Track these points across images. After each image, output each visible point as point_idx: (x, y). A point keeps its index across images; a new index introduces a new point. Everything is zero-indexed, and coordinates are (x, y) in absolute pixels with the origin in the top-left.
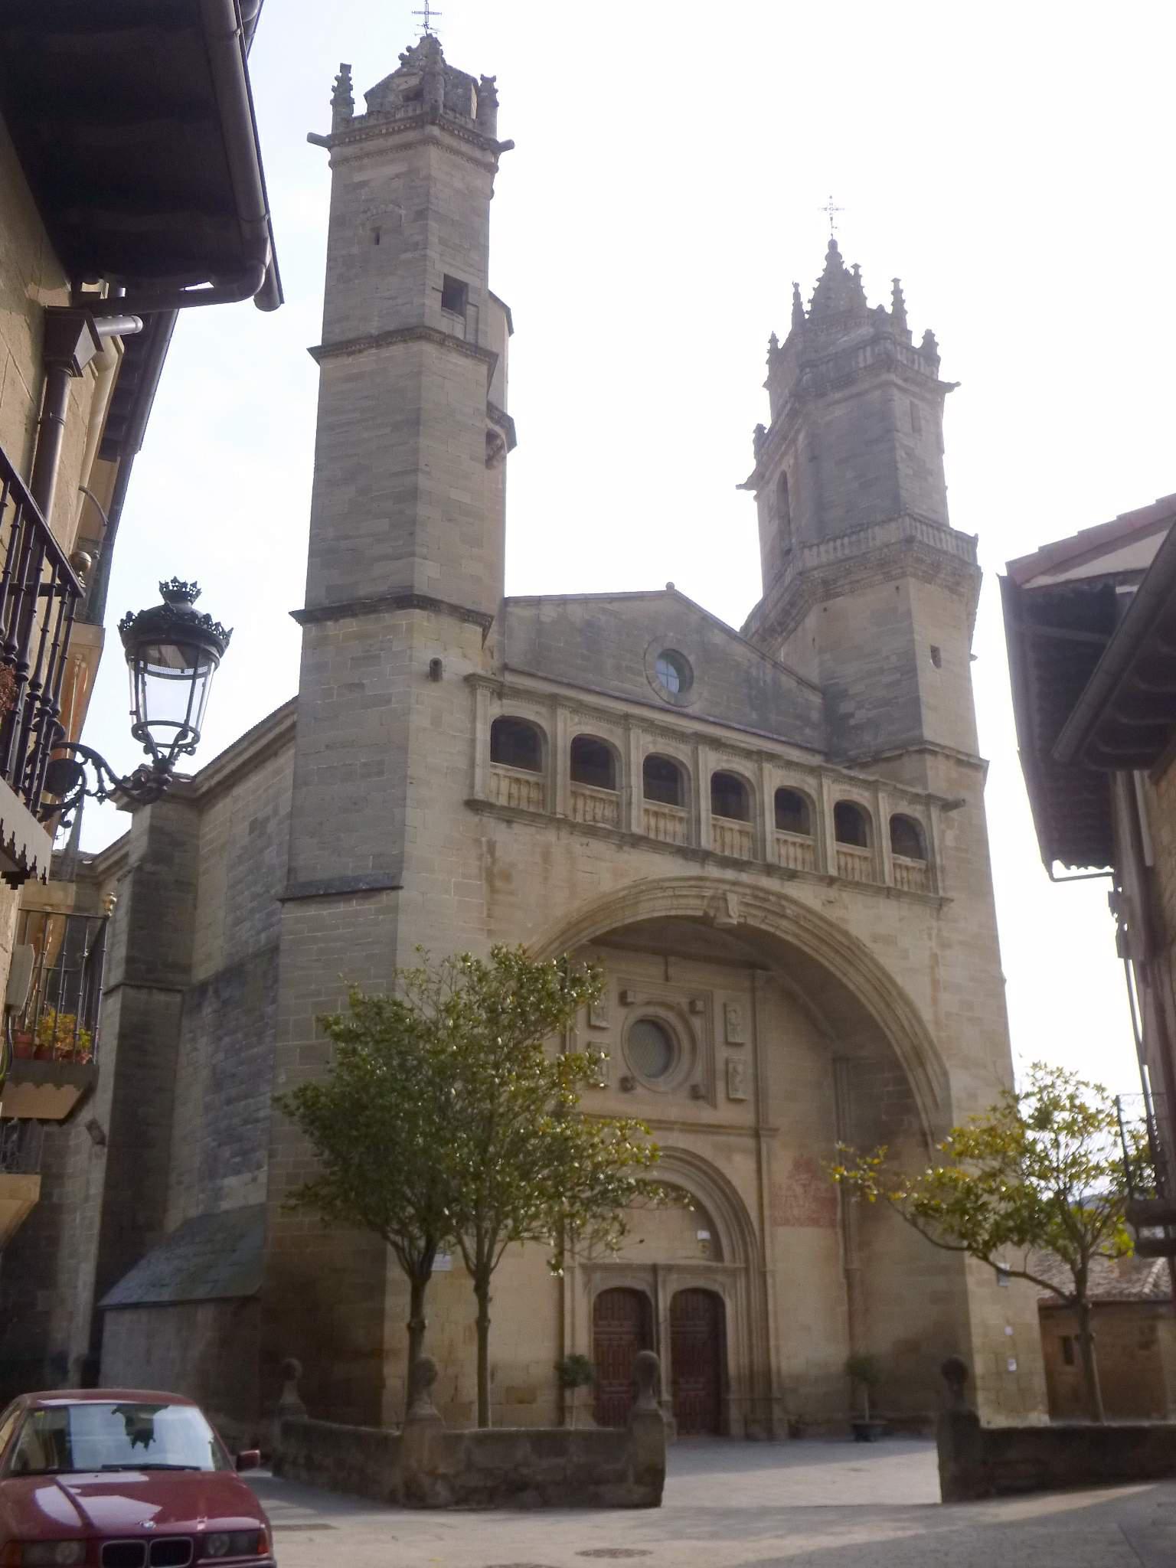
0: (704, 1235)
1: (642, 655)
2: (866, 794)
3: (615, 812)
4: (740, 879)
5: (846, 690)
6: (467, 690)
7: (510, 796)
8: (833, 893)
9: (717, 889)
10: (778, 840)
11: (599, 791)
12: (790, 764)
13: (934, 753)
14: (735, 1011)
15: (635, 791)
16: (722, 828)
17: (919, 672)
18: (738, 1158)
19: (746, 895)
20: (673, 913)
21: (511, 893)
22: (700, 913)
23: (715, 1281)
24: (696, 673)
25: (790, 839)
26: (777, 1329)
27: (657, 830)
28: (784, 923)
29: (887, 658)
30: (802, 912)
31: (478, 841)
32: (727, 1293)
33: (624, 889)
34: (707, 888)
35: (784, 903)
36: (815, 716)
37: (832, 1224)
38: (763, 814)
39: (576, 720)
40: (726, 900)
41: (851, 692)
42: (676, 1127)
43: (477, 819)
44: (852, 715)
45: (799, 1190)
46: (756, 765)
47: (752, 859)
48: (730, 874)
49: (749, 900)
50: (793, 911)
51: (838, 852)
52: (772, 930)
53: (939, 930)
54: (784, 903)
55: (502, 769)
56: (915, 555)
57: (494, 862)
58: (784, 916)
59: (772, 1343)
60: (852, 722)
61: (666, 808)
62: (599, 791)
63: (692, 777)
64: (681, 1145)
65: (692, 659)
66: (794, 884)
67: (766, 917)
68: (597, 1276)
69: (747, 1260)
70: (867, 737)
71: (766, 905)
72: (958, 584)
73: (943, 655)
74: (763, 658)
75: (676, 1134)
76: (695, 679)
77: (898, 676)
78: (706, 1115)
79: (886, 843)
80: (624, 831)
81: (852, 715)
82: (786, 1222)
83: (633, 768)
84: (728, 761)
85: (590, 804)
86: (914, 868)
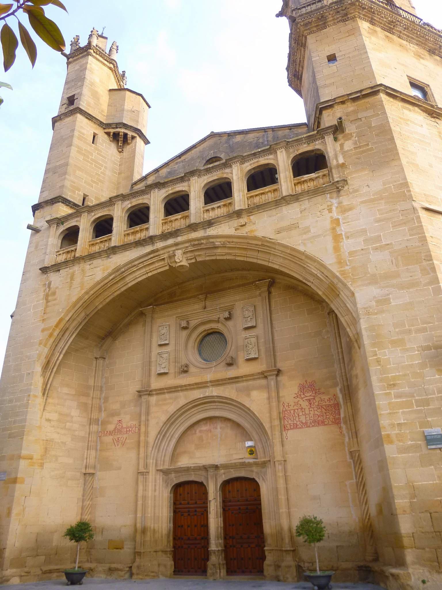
4: (177, 241)
9: (169, 252)
18: (255, 394)
19: (187, 247)
20: (150, 274)
21: (55, 299)
22: (167, 268)
23: (252, 471)
28: (219, 251)
30: (223, 240)
33: (110, 275)
35: (211, 240)
37: (337, 422)
42: (208, 385)
43: (46, 276)
45: (305, 404)
48: (171, 241)
49: (190, 249)
50: (220, 242)
52: (214, 258)
54: (211, 240)
56: (302, 24)
58: (216, 248)
64: (215, 394)
66: (214, 228)
68: (173, 475)
71: (203, 246)
72: (346, 15)
74: (265, 132)
78: (232, 373)
82: (296, 427)
84: (172, 189)
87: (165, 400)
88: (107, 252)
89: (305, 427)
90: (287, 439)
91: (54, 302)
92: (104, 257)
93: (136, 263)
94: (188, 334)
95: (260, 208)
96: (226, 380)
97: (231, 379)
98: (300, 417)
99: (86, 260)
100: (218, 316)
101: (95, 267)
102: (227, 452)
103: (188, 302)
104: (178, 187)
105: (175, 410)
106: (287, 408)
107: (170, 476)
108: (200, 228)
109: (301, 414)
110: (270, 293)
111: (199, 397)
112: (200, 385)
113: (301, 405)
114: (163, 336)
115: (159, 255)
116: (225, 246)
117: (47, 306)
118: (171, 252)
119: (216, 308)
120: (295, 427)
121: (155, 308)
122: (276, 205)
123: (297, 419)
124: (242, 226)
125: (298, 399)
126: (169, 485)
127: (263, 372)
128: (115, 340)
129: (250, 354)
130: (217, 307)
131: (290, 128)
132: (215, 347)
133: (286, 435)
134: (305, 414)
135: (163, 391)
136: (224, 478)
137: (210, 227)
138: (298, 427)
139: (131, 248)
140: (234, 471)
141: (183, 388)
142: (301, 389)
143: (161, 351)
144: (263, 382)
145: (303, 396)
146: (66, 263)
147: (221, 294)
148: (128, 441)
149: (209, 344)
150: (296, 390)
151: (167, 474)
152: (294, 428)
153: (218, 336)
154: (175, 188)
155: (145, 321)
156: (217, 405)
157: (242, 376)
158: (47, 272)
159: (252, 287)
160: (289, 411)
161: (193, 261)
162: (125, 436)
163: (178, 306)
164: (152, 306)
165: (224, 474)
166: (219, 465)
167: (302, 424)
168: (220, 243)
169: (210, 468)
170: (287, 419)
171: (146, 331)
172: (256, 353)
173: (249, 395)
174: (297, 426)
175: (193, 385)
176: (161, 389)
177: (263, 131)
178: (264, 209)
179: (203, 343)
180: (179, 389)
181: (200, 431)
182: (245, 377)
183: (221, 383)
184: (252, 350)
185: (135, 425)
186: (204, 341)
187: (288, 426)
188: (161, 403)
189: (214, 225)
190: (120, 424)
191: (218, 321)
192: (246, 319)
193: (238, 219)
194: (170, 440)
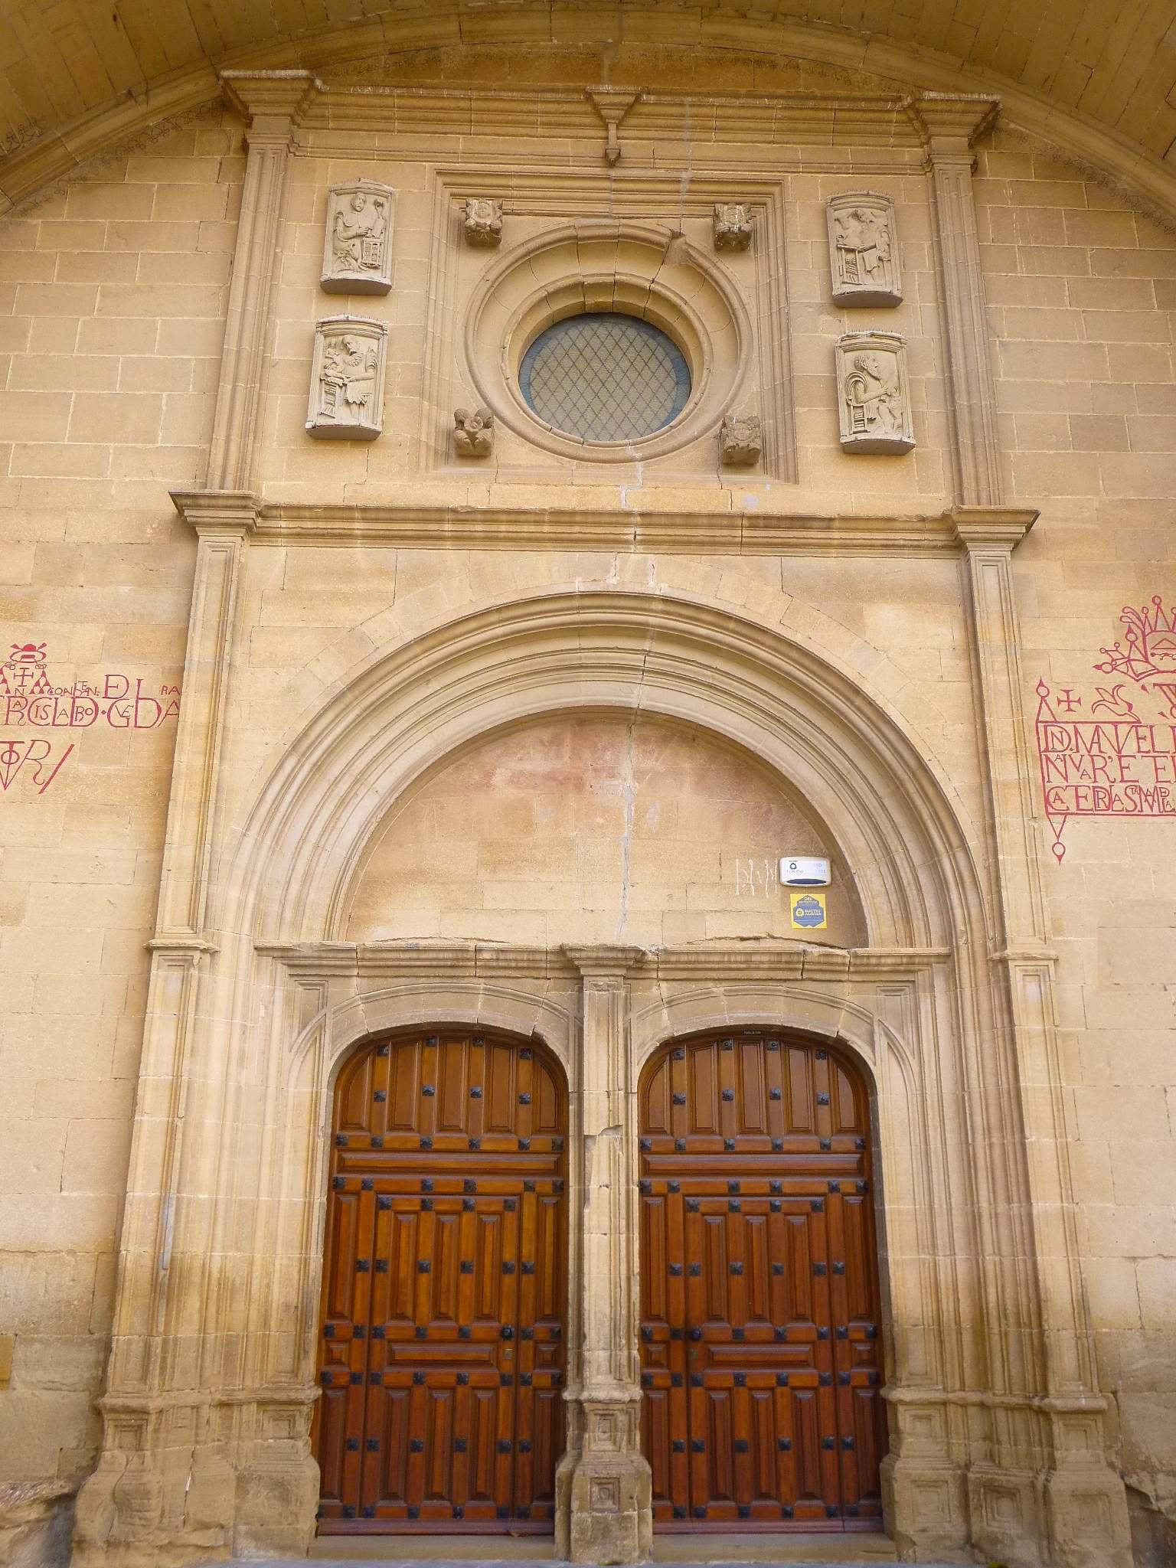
0: (814, 868)
14: (856, 216)
23: (833, 1004)
26: (1064, 1156)
32: (881, 1042)
42: (628, 533)
59: (1046, 1204)
69: (949, 934)
75: (635, 557)
82: (1103, 804)
87: (349, 574)
89: (1156, 811)
90: (1060, 857)
94: (491, 277)
96: (732, 527)
97: (766, 527)
98: (1125, 762)
100: (672, 224)
102: (670, 896)
103: (525, 107)
105: (410, 635)
106: (1060, 711)
107: (334, 988)
109: (1130, 747)
110: (975, 167)
111: (562, 589)
112: (576, 529)
113: (1130, 706)
114: (357, 241)
119: (673, 174)
120: (1102, 806)
121: (320, 92)
123: (1113, 769)
125: (1116, 678)
126: (327, 1039)
127: (955, 518)
128: (25, 212)
129: (871, 420)
130: (684, 175)
132: (611, 386)
133: (1058, 837)
134: (1154, 753)
135: (346, 525)
136: (668, 1025)
138: (1117, 806)
140: (728, 994)
141: (468, 527)
142: (1130, 631)
143: (342, 317)
144: (940, 570)
145: (1140, 667)
147: (714, 111)
148: (84, 768)
149: (582, 364)
150: (1106, 632)
151: (316, 980)
152: (1094, 812)
153: (632, 333)
155: (245, 147)
156: (648, 653)
157: (831, 520)
159: (886, 116)
160: (1070, 728)
162: (60, 738)
163: (455, 116)
164: (302, 73)
165: (671, 1003)
166: (650, 957)
167: (1136, 797)
169: (599, 963)
170: (1060, 764)
171: (250, 196)
172: (901, 426)
173: (853, 622)
174: (1111, 802)
175: (536, 516)
176: (331, 512)
179: (545, 352)
180: (447, 527)
181: (516, 780)
182: (841, 529)
183: (701, 533)
184: (883, 407)
185: (133, 682)
186: (553, 344)
187: (1068, 796)
188: (318, 587)
190: (32, 668)
191: (656, 250)
192: (850, 256)
194: (343, 803)
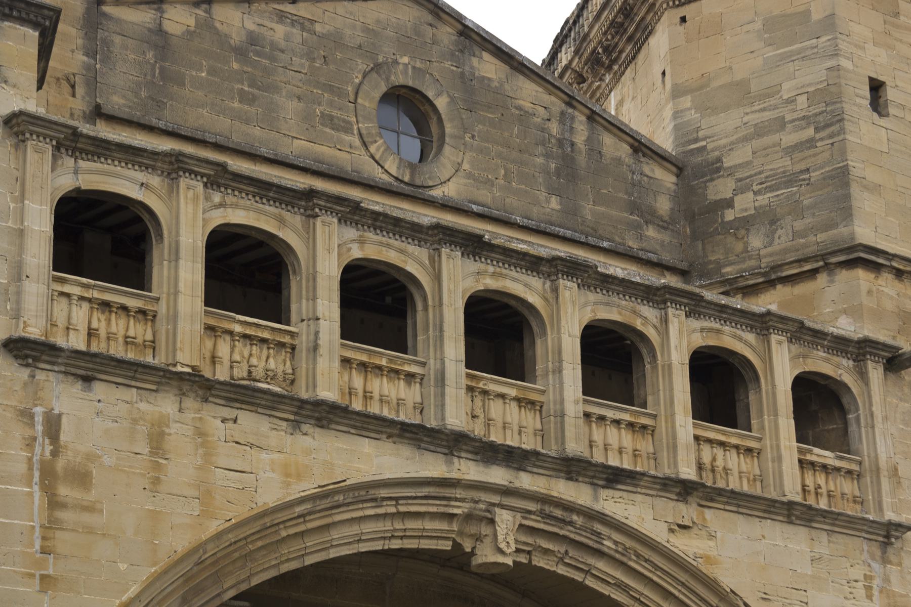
1: (352, 99)
2: (750, 337)
3: (288, 363)
5: (719, 160)
6: (14, 140)
7: (91, 333)
8: (688, 512)
9: (477, 502)
10: (587, 415)
11: (258, 326)
12: (606, 282)
13: (876, 268)
15: (324, 325)
16: (485, 393)
17: (848, 125)
19: (529, 512)
21: (89, 508)
22: (447, 546)
24: (449, 129)
25: (610, 414)
27: (367, 396)
29: (791, 101)
30: (629, 543)
31: (27, 416)
34: (456, 499)
36: (664, 205)
38: (559, 371)
39: (217, 198)
40: (492, 521)
41: (728, 162)
43: (25, 373)
44: (729, 204)
46: (548, 284)
47: (539, 449)
48: (498, 475)
50: (616, 543)
51: (697, 438)
52: (578, 577)
53: (887, 580)
54: (598, 527)
55: (75, 285)
57: (55, 453)
58: (599, 554)
60: (729, 215)
61: (383, 357)
62: (258, 326)
63: (430, 303)
65: (441, 103)
66: (618, 494)
67: (567, 552)
70: (756, 241)
73: (891, 94)
76: (447, 140)
77: (810, 132)
79: (787, 425)
80: (304, 395)
81: (729, 204)
83: (321, 283)
84: (494, 275)
85: (242, 350)
86: (838, 470)
88: (300, 408)
91: (87, 518)
92: (281, 419)
93: (384, 493)
95: (734, 498)
99: (213, 396)
101: (252, 446)
104: (514, 280)
108: (585, 476)
115: (449, 499)
116: (624, 559)
117: (51, 526)
118: (482, 506)
122: (765, 511)
124: (682, 527)
131: (636, 144)
137: (608, 488)
139: (382, 432)
146: (140, 370)
154: (504, 276)
158: (36, 359)
161: (523, 559)
168: (614, 547)
177: (567, 99)
178: (739, 506)
189: (619, 487)
193: (677, 500)
